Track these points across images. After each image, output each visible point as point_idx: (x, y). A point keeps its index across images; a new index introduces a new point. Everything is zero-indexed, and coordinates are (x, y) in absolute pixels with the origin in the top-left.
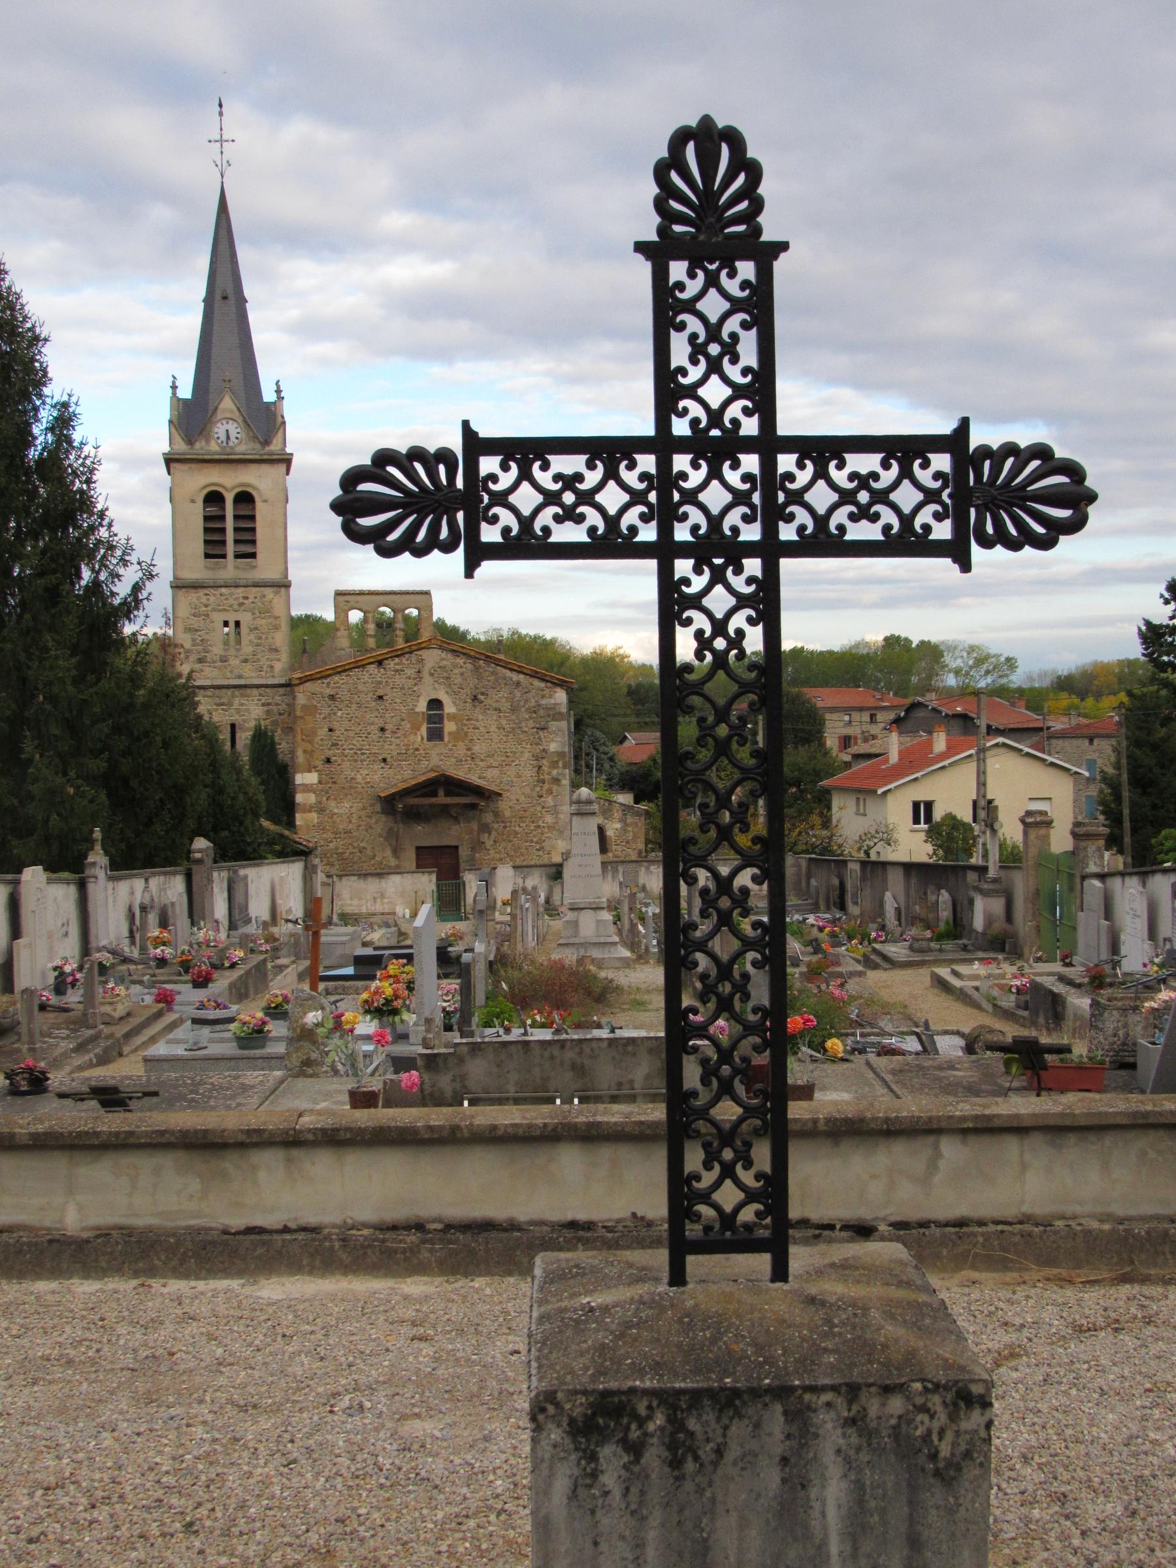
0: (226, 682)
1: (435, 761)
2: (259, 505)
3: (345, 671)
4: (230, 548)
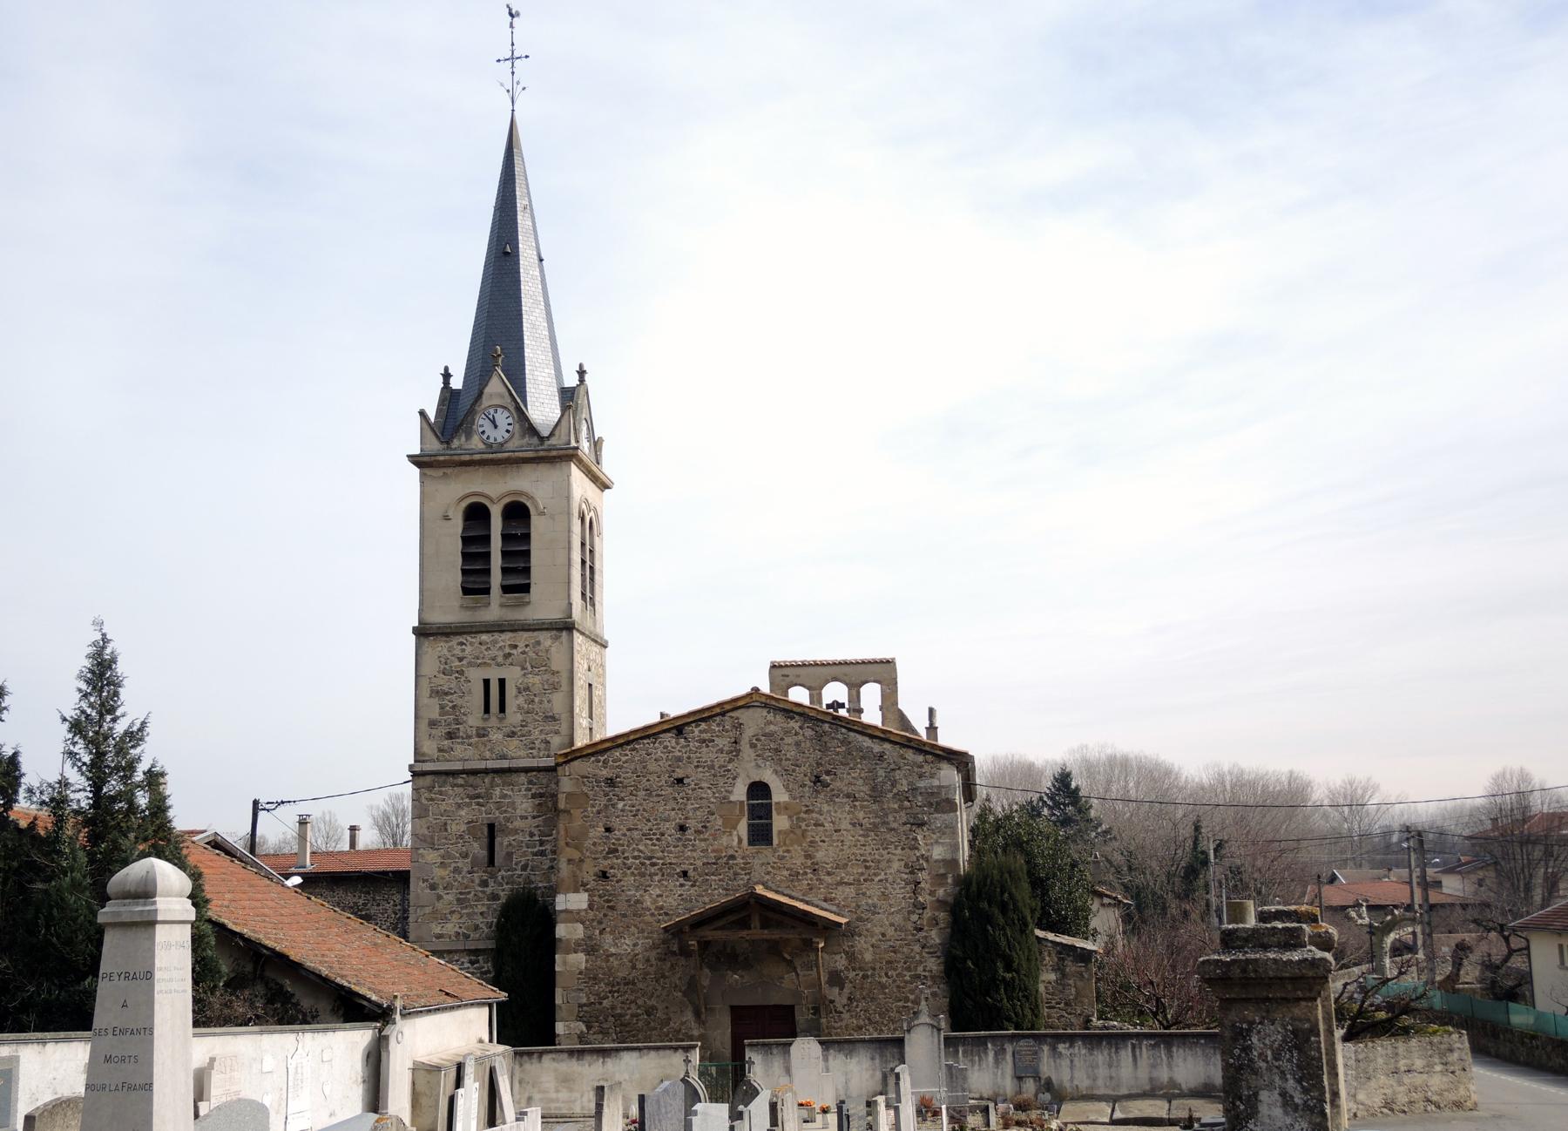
0: (482, 765)
2: (535, 521)
3: (628, 743)
4: (496, 578)
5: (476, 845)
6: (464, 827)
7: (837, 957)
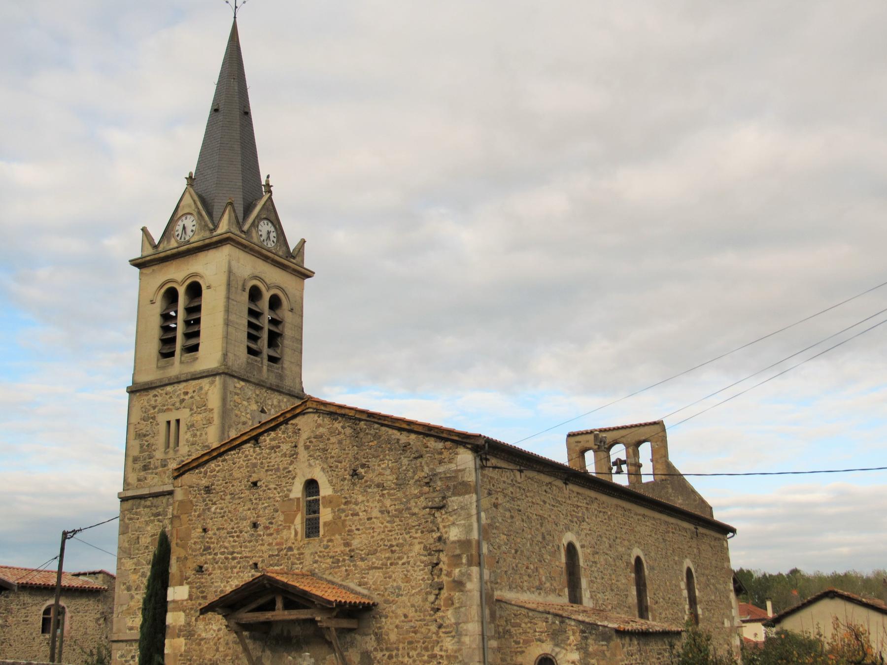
3: (220, 455)
7: (367, 639)
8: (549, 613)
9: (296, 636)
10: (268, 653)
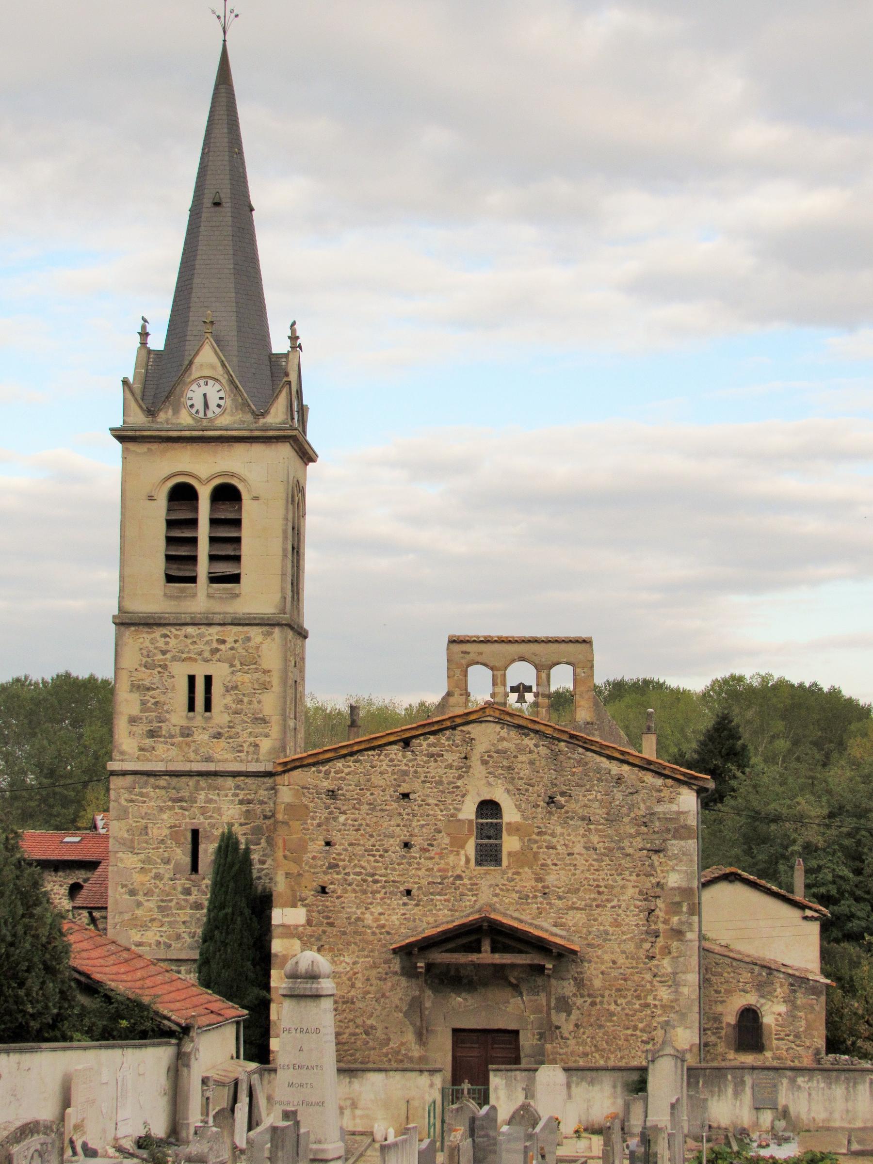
0: (187, 767)
1: (485, 896)
3: (352, 754)
4: (203, 567)
5: (179, 851)
6: (166, 832)
7: (565, 983)
8: (756, 964)
9: (467, 976)
10: (429, 992)
